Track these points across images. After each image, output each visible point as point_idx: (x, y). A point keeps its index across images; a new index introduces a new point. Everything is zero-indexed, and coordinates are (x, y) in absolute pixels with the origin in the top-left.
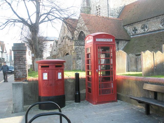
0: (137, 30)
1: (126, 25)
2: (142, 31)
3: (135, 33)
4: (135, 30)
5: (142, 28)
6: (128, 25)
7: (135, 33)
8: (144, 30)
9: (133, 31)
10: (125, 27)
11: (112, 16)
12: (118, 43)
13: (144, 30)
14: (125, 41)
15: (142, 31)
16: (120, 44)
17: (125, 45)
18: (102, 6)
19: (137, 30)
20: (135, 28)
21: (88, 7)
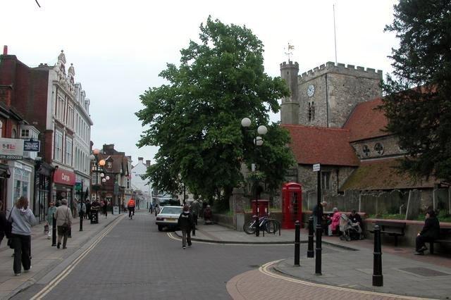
0: (369, 151)
1: (354, 142)
2: (376, 153)
3: (367, 154)
4: (367, 150)
5: (377, 149)
6: (357, 142)
7: (367, 154)
8: (379, 153)
9: (364, 151)
10: (352, 144)
11: (334, 122)
12: (338, 172)
13: (379, 153)
14: (349, 169)
15: (376, 153)
16: (341, 173)
17: (350, 174)
18: (317, 105)
19: (369, 151)
20: (366, 147)
21: (294, 102)
